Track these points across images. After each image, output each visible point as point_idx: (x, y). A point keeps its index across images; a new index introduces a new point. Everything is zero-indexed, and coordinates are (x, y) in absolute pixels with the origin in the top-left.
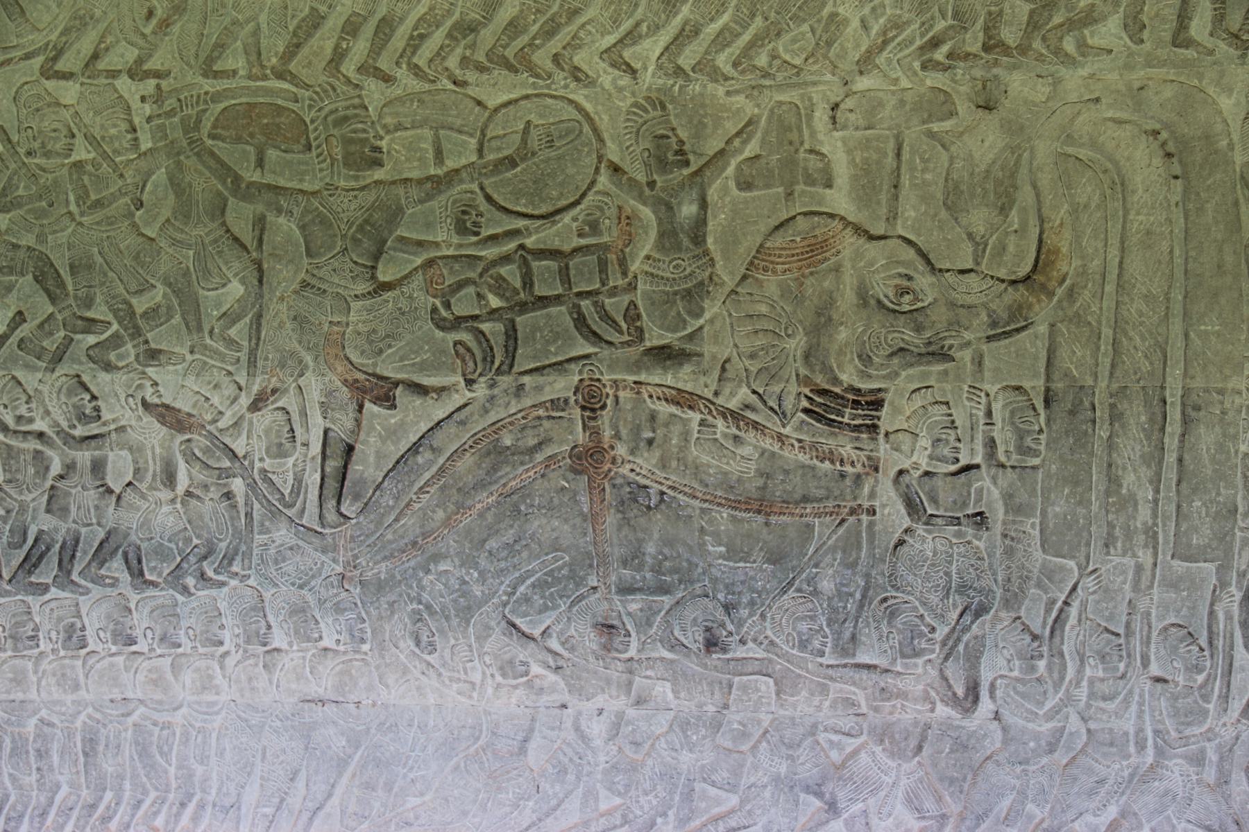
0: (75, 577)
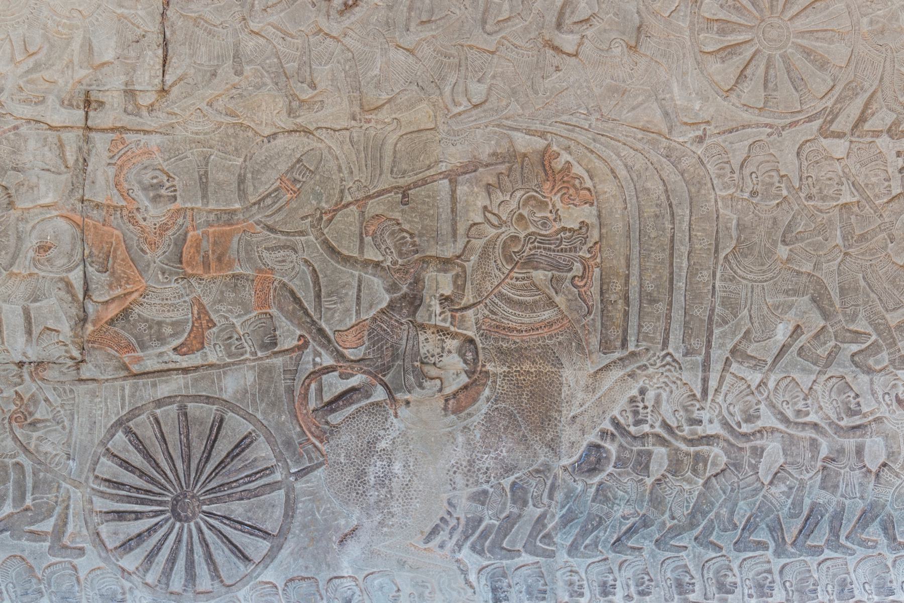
0: (842, 540)
